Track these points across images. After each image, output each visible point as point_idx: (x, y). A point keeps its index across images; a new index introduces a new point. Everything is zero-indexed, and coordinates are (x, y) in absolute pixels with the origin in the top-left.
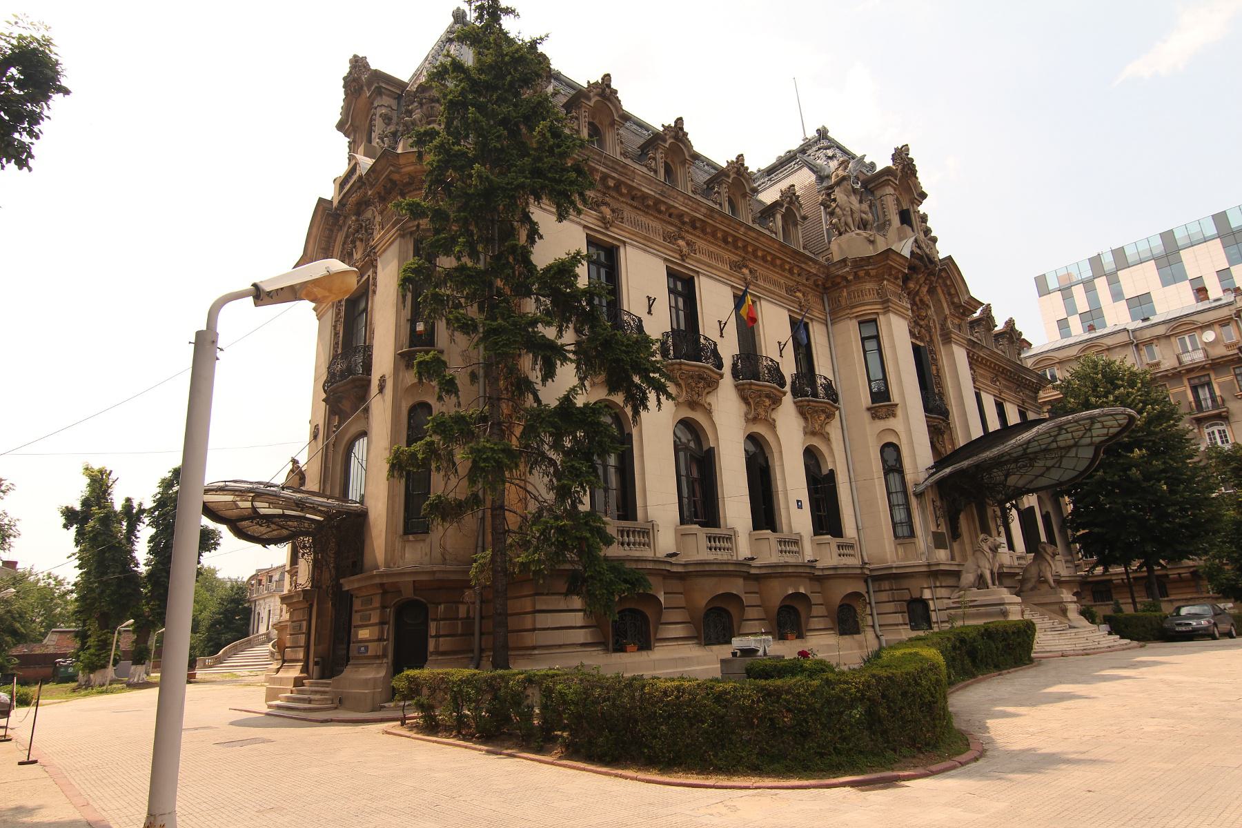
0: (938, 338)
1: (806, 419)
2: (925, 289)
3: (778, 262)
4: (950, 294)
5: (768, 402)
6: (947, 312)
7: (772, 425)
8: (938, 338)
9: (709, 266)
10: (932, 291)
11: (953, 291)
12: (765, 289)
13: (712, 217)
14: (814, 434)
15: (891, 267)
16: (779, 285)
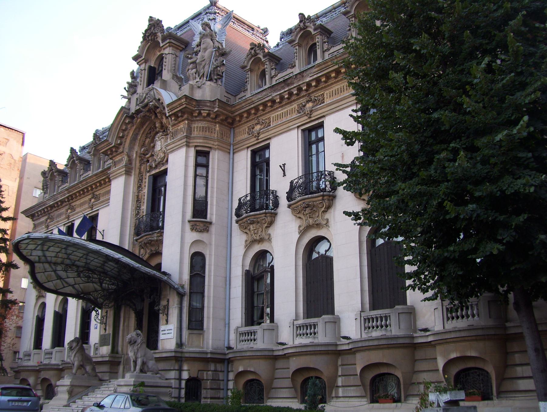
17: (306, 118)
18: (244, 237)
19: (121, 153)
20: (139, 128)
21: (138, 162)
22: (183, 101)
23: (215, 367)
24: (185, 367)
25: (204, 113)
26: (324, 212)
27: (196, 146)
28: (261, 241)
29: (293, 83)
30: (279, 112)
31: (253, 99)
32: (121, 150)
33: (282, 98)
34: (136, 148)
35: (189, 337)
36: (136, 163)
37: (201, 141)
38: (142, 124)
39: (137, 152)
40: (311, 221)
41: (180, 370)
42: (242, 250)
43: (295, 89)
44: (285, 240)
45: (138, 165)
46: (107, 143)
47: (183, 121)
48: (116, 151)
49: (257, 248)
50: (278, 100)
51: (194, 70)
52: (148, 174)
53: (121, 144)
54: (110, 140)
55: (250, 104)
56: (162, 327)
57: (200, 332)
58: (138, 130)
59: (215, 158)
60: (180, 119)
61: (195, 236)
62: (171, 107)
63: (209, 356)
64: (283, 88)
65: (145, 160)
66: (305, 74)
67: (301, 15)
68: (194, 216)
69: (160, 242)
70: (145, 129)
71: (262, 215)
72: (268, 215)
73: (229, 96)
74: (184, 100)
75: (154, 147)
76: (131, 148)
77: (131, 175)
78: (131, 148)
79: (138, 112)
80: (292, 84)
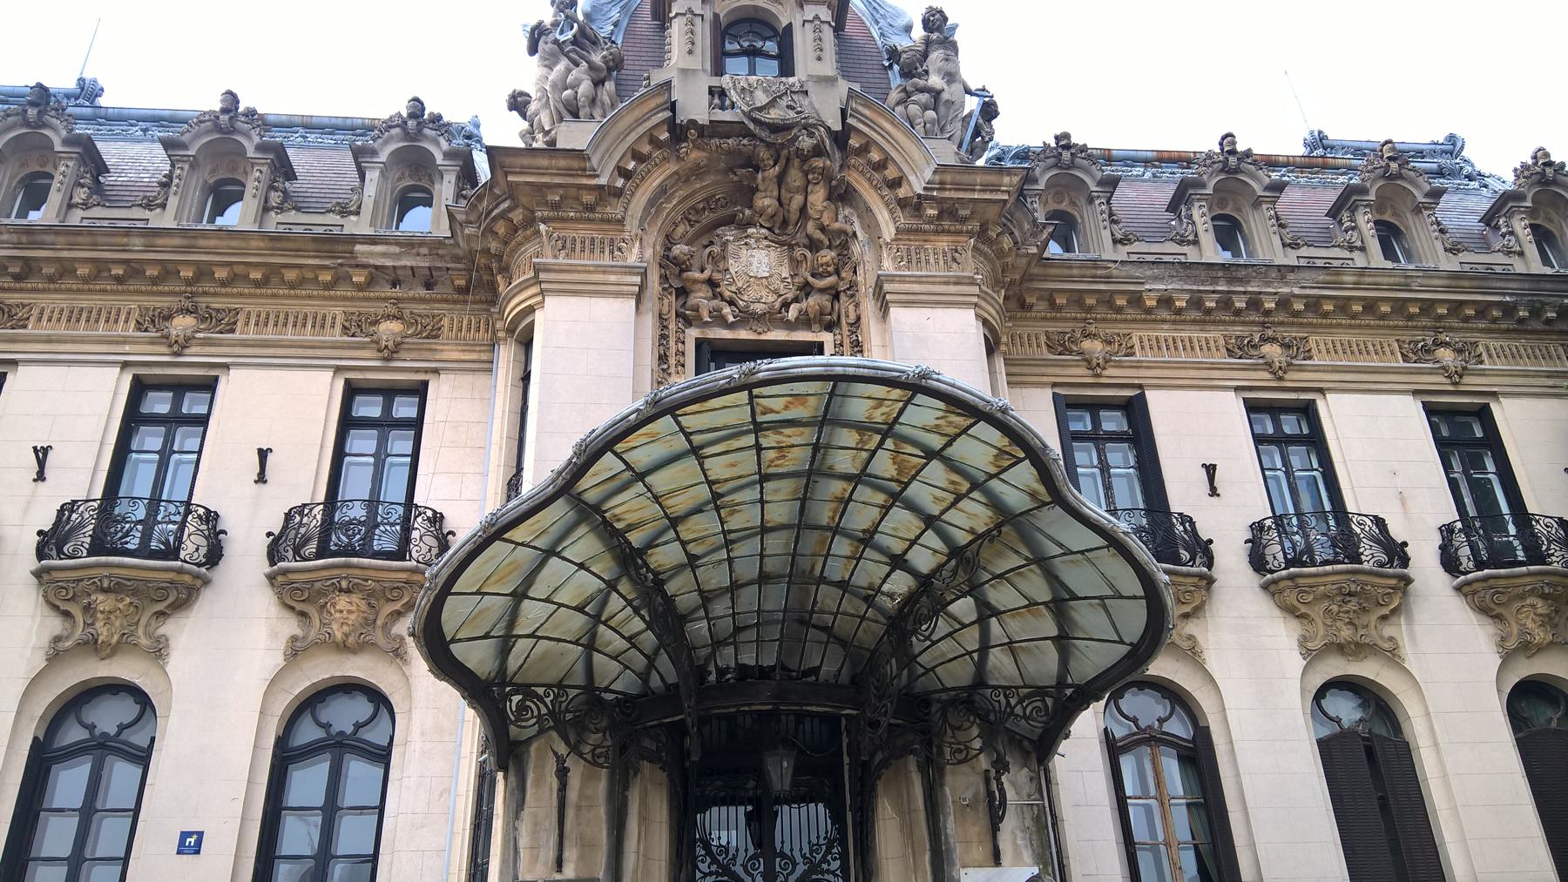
0: (869, 308)
1: (303, 614)
2: (818, 197)
3: (290, 275)
4: (896, 183)
5: (103, 602)
6: (888, 232)
7: (158, 652)
8: (869, 308)
9: (49, 340)
10: (842, 195)
11: (891, 173)
12: (244, 344)
13: (41, 246)
14: (343, 648)
15: (540, 188)
16: (321, 323)
17: (1267, 375)
19: (609, 221)
20: (682, 178)
22: (1006, 180)
26: (1384, 618)
29: (1248, 282)
30: (1164, 332)
32: (614, 209)
33: (1196, 302)
38: (697, 171)
40: (1346, 633)
43: (1245, 298)
46: (575, 164)
47: (959, 233)
48: (590, 208)
51: (931, 114)
52: (693, 333)
54: (595, 161)
55: (1095, 279)
60: (946, 224)
62: (948, 178)
64: (1215, 280)
65: (677, 284)
66: (1291, 276)
67: (231, 98)
70: (694, 193)
71: (1189, 580)
72: (1282, 584)
74: (1016, 179)
79: (715, 129)
80: (1241, 281)
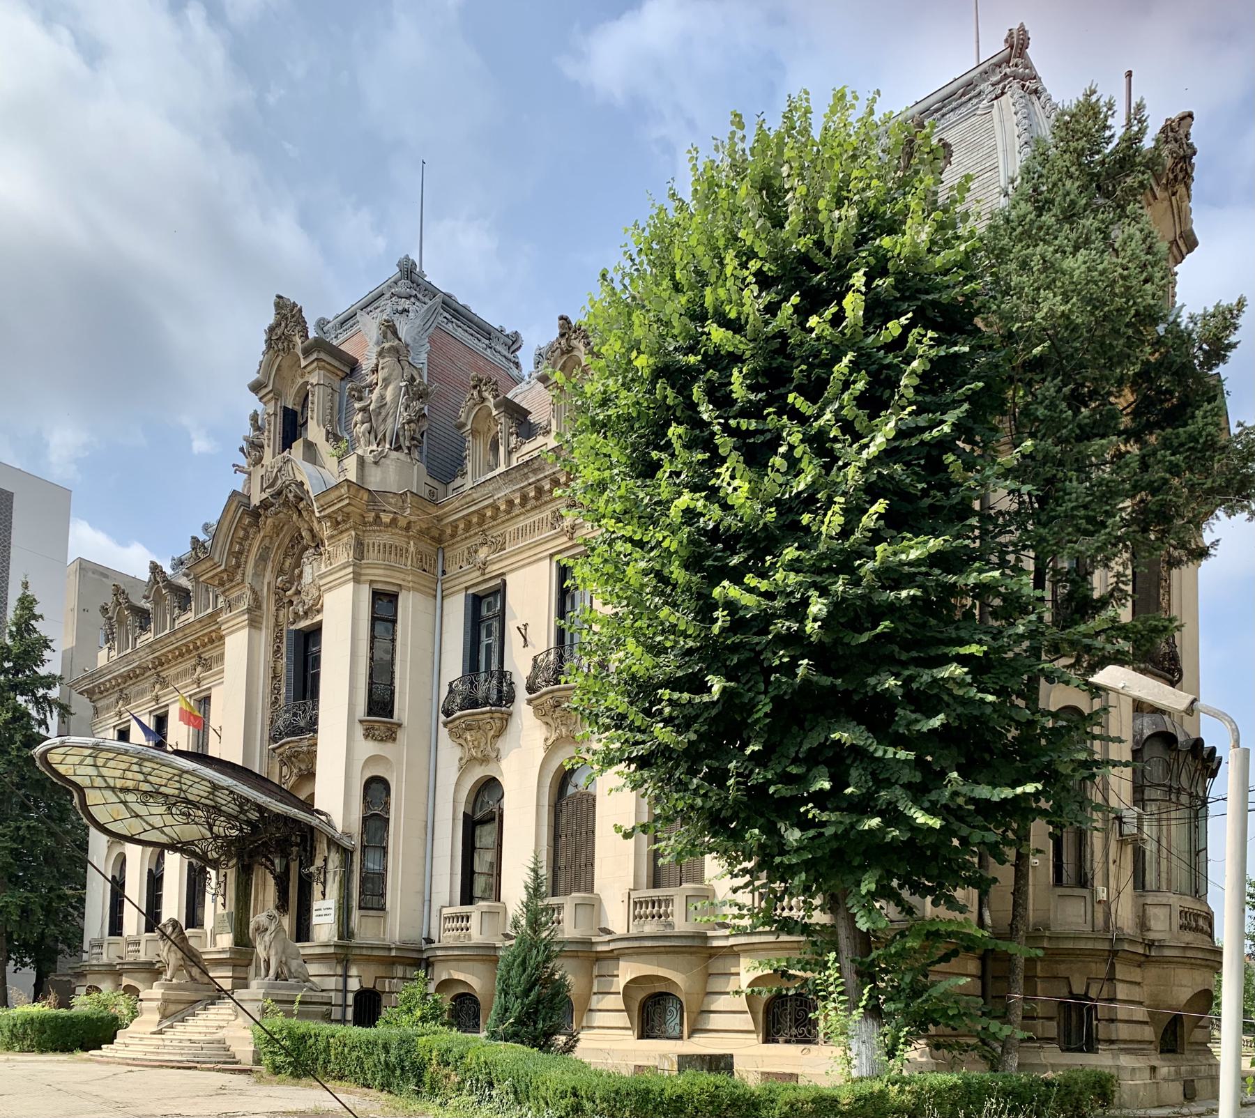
17: (565, 539)
18: (458, 753)
21: (272, 601)
23: (405, 972)
24: (354, 971)
25: (386, 518)
27: (371, 582)
28: (485, 760)
30: (521, 523)
31: (475, 496)
32: (238, 578)
34: (269, 576)
35: (360, 922)
36: (269, 606)
37: (381, 572)
39: (269, 584)
41: (346, 976)
42: (454, 775)
43: (547, 481)
44: (523, 760)
45: (273, 608)
49: (478, 773)
50: (517, 501)
53: (238, 565)
56: (316, 905)
57: (381, 913)
58: (267, 540)
59: (408, 606)
61: (368, 748)
63: (393, 953)
65: (286, 600)
68: (370, 712)
69: (312, 755)
73: (435, 484)
75: (300, 575)
76: (258, 574)
77: (260, 629)
78: (258, 574)
